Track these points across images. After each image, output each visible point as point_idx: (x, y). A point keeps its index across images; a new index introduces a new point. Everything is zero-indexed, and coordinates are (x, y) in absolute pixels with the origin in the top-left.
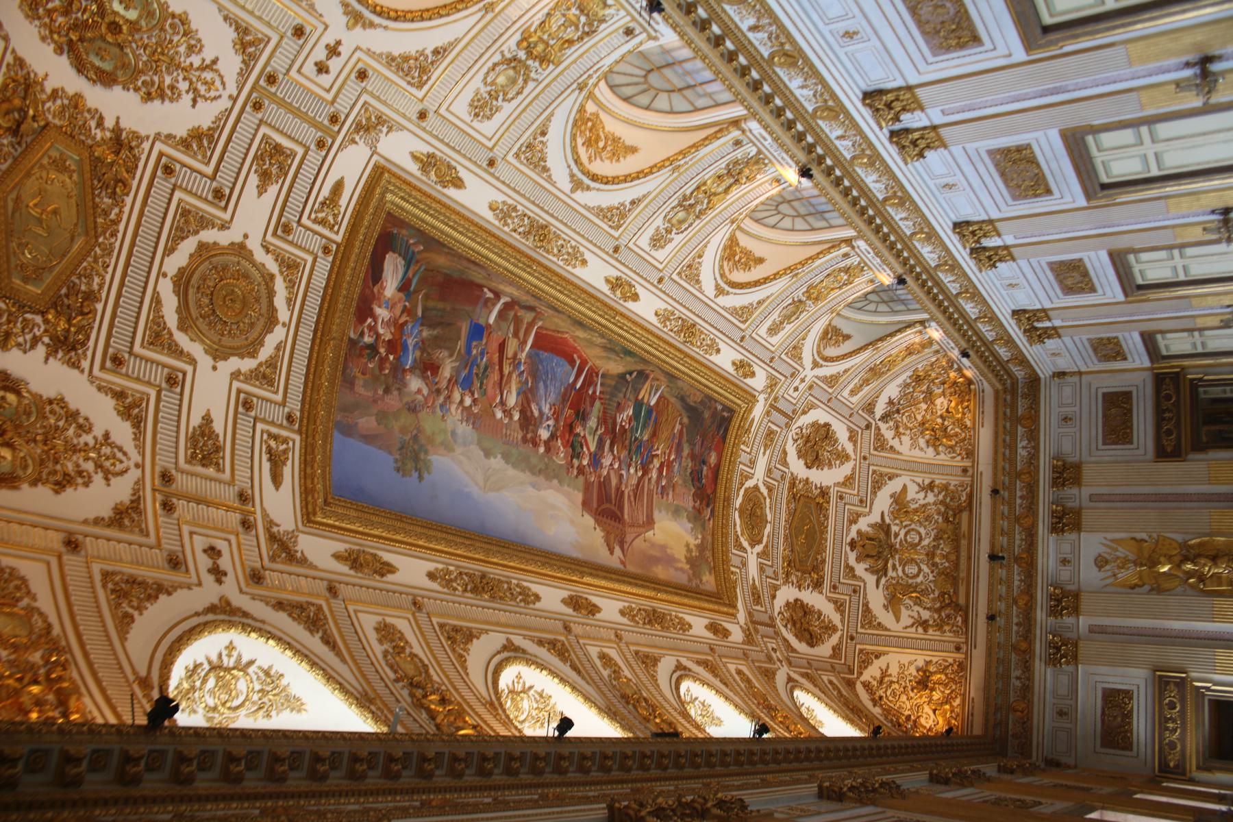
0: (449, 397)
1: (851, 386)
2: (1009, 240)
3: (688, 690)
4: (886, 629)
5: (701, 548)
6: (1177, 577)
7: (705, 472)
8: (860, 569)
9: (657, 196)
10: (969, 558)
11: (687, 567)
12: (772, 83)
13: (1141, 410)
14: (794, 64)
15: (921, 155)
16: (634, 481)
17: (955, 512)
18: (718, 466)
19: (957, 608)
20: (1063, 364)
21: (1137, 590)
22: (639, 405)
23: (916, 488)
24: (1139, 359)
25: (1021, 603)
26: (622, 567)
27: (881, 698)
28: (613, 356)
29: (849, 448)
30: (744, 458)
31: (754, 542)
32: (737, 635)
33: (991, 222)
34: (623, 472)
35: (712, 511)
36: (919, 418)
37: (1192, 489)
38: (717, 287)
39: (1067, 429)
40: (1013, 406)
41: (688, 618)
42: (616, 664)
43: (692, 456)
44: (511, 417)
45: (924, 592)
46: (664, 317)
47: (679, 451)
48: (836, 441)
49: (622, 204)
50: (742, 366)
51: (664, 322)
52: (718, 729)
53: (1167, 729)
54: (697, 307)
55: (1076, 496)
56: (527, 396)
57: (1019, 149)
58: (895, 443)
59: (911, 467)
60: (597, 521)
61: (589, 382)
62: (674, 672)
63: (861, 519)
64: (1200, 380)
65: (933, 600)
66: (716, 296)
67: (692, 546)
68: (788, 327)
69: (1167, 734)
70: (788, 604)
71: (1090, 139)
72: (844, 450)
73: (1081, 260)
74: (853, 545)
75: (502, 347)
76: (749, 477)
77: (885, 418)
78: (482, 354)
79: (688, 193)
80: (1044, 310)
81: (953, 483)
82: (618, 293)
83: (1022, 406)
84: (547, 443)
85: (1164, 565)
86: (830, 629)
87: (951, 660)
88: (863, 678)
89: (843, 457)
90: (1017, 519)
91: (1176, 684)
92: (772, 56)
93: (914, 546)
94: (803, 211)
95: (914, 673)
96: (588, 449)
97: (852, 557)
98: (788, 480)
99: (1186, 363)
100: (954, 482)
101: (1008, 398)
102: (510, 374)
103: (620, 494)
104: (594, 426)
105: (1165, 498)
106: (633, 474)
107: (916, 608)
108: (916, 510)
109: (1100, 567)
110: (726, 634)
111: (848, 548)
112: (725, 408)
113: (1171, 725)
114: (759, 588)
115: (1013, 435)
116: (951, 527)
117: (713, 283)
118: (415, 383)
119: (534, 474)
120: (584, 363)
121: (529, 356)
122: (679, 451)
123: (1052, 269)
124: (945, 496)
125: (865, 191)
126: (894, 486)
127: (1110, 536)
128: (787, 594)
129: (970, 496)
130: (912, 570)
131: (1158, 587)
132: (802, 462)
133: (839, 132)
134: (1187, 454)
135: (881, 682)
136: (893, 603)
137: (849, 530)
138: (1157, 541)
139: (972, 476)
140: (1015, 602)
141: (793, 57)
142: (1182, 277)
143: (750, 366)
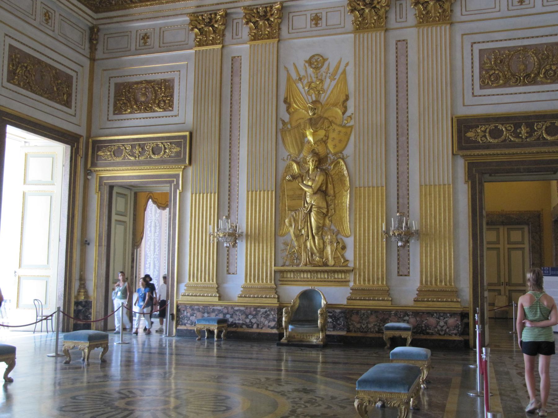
6: (300, 151)
13: (536, 97)
21: (283, 107)
69: (129, 148)
85: (314, 135)
91: (178, 154)
105: (402, 132)
109: (310, 62)
113: (137, 151)
127: (350, 70)
134: (463, 156)
138: (344, 126)
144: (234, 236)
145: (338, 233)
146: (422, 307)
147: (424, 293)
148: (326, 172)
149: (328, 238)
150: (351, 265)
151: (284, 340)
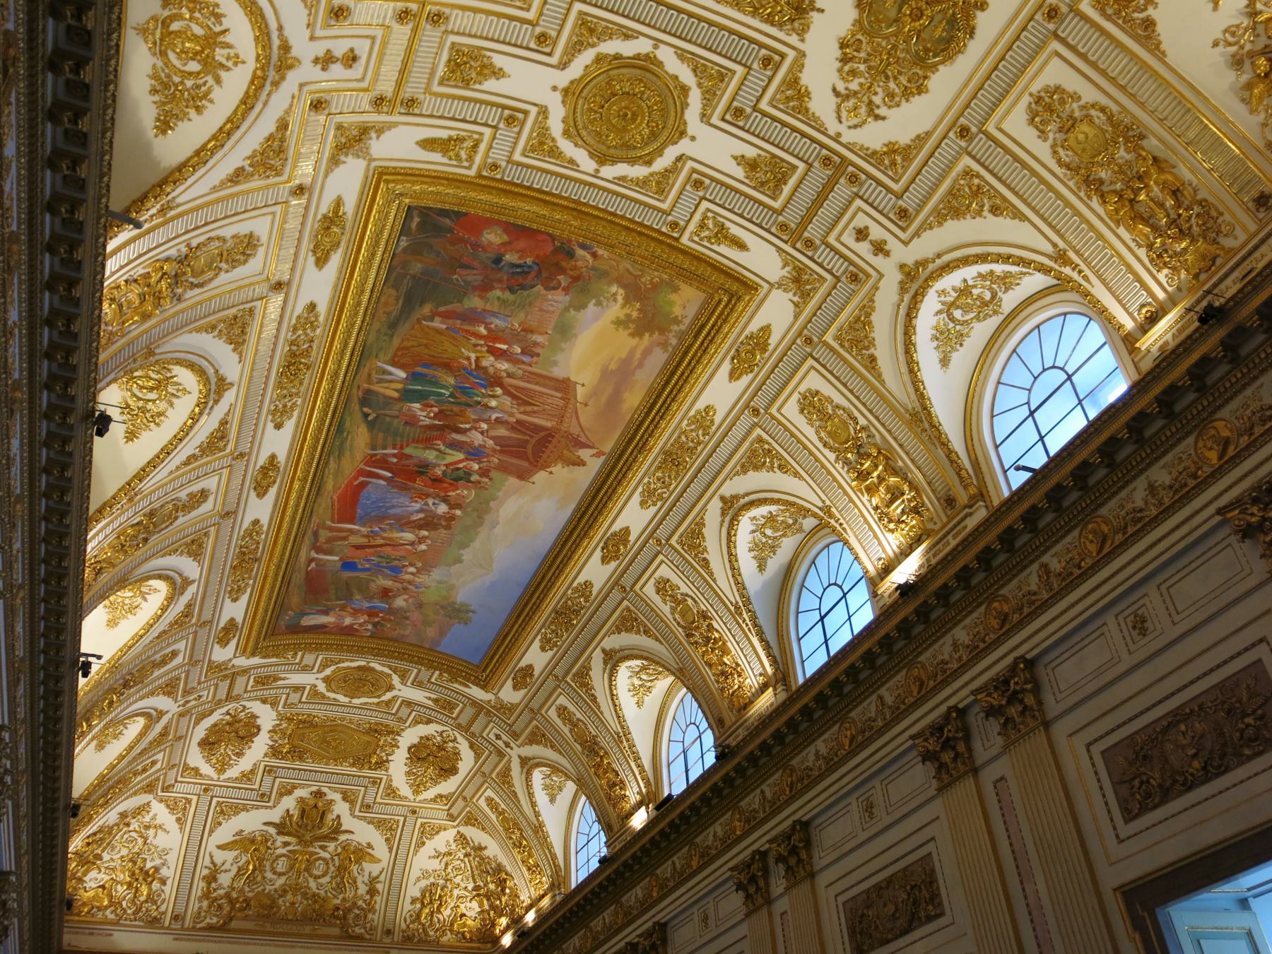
0: (409, 582)
5: (635, 292)
16: (507, 401)
18: (508, 227)
34: (494, 416)
35: (583, 247)
43: (485, 288)
44: (427, 537)
47: (472, 317)
56: (404, 523)
60: (544, 467)
61: (383, 463)
75: (358, 547)
78: (368, 560)
84: (452, 507)
96: (460, 461)
102: (384, 538)
103: (519, 426)
104: (435, 453)
106: (498, 402)
117: (216, 408)
118: (400, 602)
119: (482, 524)
120: (361, 473)
121: (363, 525)
122: (472, 317)
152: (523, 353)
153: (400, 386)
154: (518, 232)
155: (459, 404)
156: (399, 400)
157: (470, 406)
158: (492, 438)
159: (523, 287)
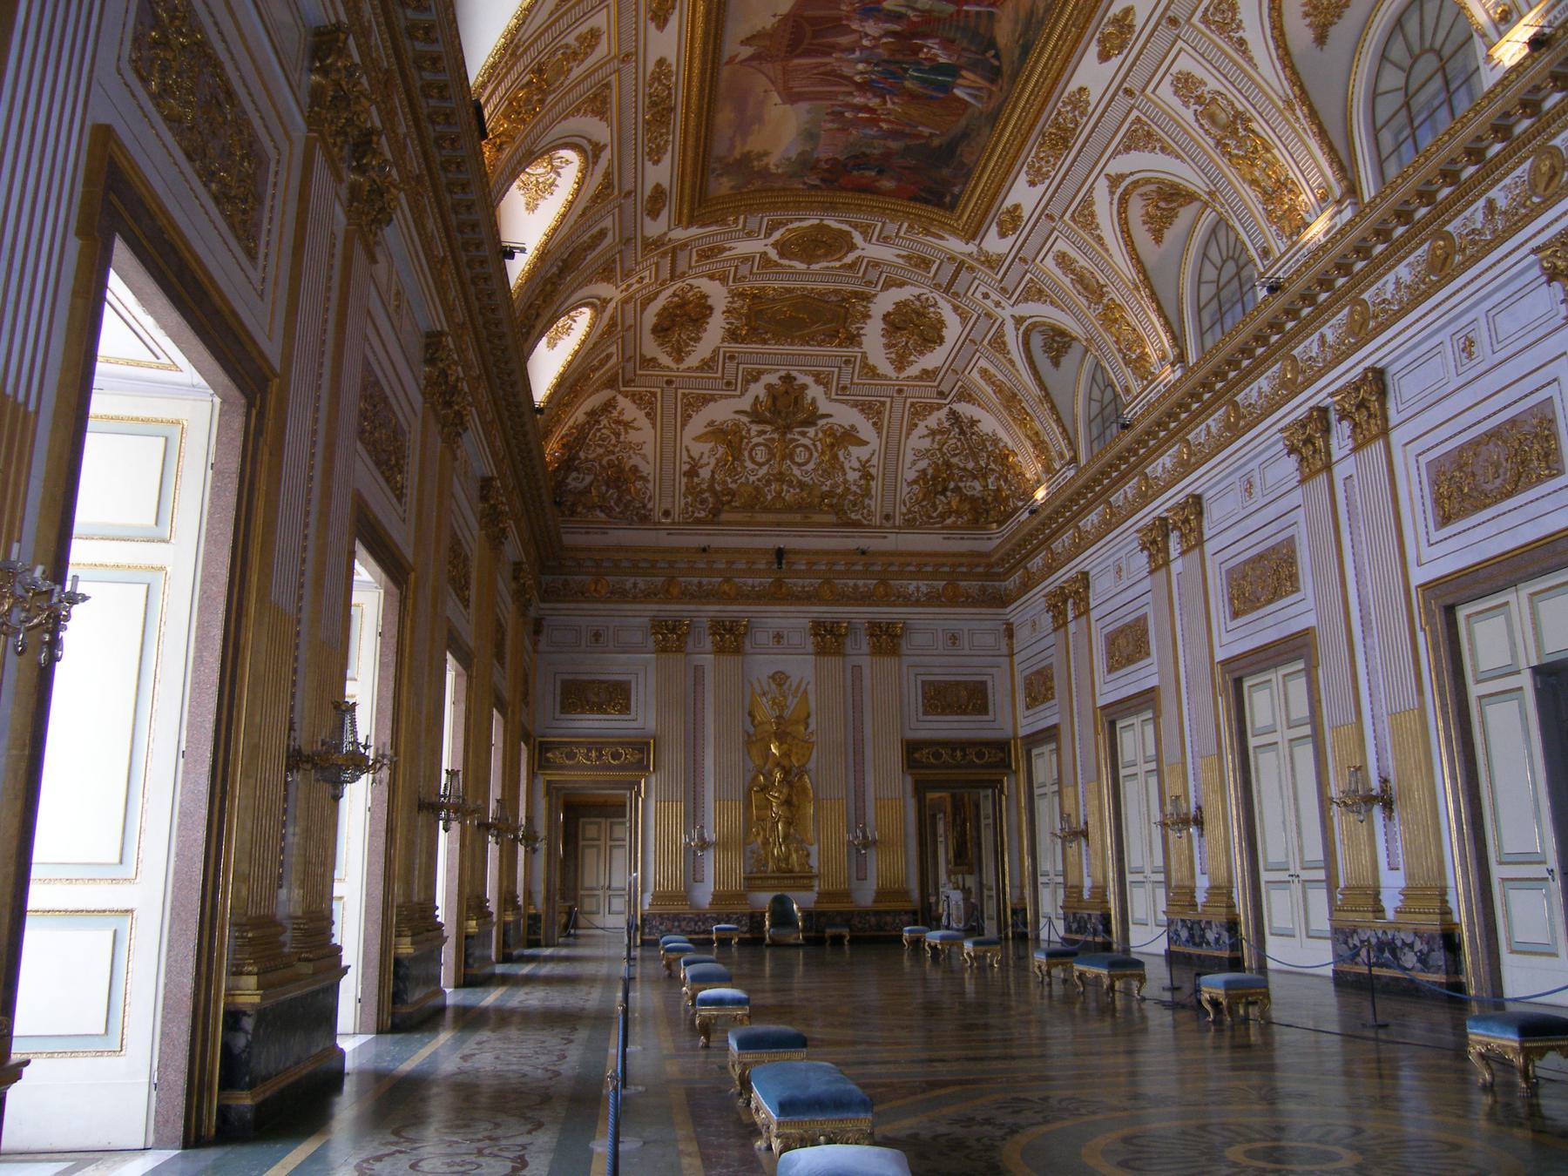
1: (992, 370)
2: (1176, 567)
3: (568, 162)
4: (683, 426)
5: (765, 174)
7: (867, 173)
8: (758, 389)
9: (1251, 78)
10: (778, 525)
11: (737, 154)
12: (1407, 239)
14: (1431, 268)
15: (1292, 450)
16: (847, 71)
17: (839, 508)
19: (716, 512)
20: (1023, 635)
21: (748, 720)
22: (953, 71)
23: (864, 459)
24: (1028, 722)
25: (726, 587)
26: (725, 58)
27: (598, 422)
28: (1019, 28)
29: (913, 370)
30: (891, 228)
31: (783, 248)
32: (654, 228)
33: (1200, 542)
34: (858, 53)
36: (954, 460)
37: (870, 778)
38: (1122, 177)
39: (942, 639)
40: (969, 576)
41: (667, 158)
42: (586, 55)
43: (888, 154)
45: (732, 472)
46: (1079, 101)
47: (893, 134)
48: (922, 353)
49: (1239, 27)
50: (1013, 219)
51: (1071, 102)
52: (523, 207)
53: (590, 750)
54: (1091, 152)
55: (858, 649)
57: (1293, 578)
58: (922, 429)
59: (892, 452)
60: (786, 18)
62: (589, 141)
63: (821, 388)
64: (1001, 792)
65: (725, 482)
66: (1107, 176)
67: (765, 160)
68: (1067, 281)
70: (706, 297)
71: (1300, 665)
72: (911, 363)
73: (1148, 654)
74: (788, 379)
76: (866, 232)
77: (953, 413)
79: (1254, 125)
80: (1087, 611)
81: (872, 503)
82: (1111, 29)
83: (971, 586)
85: (779, 748)
86: (679, 354)
87: (650, 506)
88: (620, 398)
89: (901, 363)
90: (828, 581)
92: (1448, 237)
93: (791, 456)
94: (1225, 294)
95: (632, 462)
97: (773, 379)
98: (866, 289)
99: (1022, 776)
100: (873, 504)
101: (981, 570)
103: (827, 50)
106: (858, 69)
107: (713, 461)
108: (835, 457)
109: (773, 677)
110: (654, 214)
111: (783, 373)
112: (956, 199)
114: (721, 257)
115: (934, 575)
116: (817, 500)
122: (893, 134)
123: (1138, 619)
124: (855, 494)
125: (1248, 376)
126: (865, 430)
127: (811, 688)
128: (718, 295)
129: (857, 524)
130: (761, 454)
131: (753, 741)
132: (891, 308)
133: (1330, 338)
135: (618, 422)
136: (718, 433)
137: (806, 373)
139: (881, 527)
140: (728, 580)
141: (1442, 269)
142: (1122, 772)
143: (1015, 229)
144: (704, 845)
145: (802, 841)
146: (881, 907)
147: (881, 895)
148: (791, 785)
149: (793, 846)
150: (815, 871)
151: (768, 940)
152: (842, 113)
153: (960, 81)
154: (869, 189)
155: (897, 62)
156: (961, 67)
157: (884, 61)
158: (855, 31)
159: (856, 157)
